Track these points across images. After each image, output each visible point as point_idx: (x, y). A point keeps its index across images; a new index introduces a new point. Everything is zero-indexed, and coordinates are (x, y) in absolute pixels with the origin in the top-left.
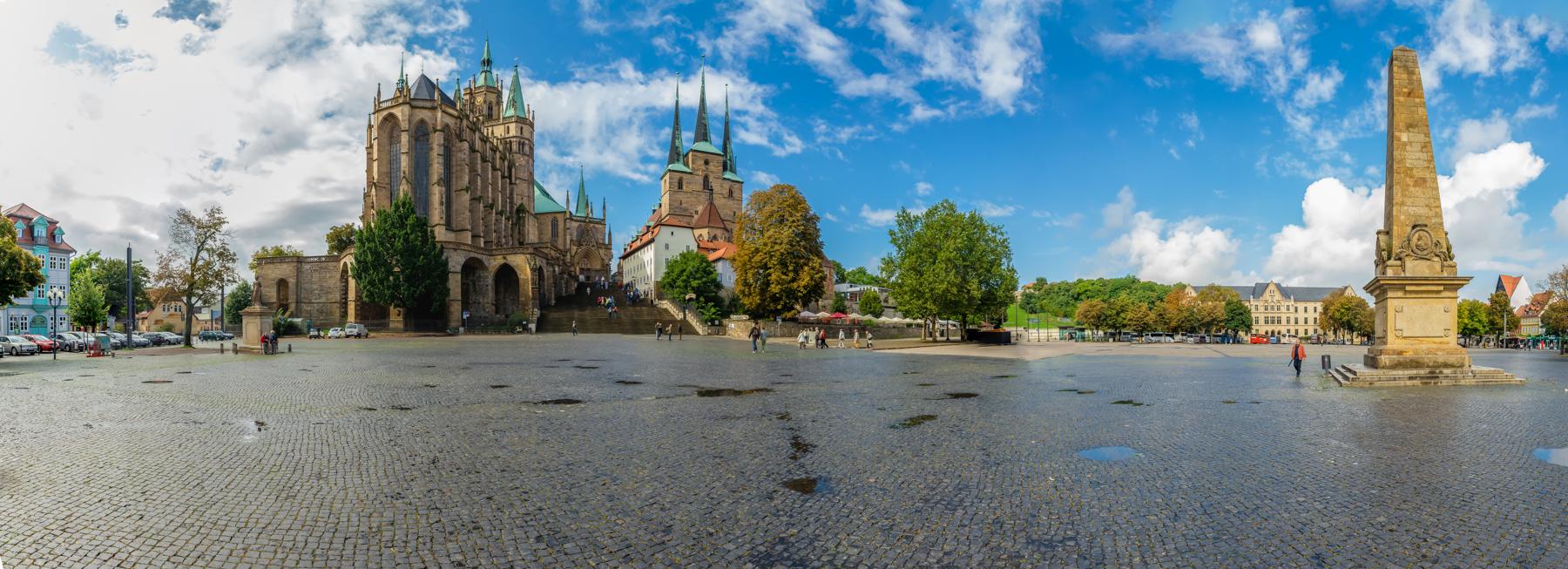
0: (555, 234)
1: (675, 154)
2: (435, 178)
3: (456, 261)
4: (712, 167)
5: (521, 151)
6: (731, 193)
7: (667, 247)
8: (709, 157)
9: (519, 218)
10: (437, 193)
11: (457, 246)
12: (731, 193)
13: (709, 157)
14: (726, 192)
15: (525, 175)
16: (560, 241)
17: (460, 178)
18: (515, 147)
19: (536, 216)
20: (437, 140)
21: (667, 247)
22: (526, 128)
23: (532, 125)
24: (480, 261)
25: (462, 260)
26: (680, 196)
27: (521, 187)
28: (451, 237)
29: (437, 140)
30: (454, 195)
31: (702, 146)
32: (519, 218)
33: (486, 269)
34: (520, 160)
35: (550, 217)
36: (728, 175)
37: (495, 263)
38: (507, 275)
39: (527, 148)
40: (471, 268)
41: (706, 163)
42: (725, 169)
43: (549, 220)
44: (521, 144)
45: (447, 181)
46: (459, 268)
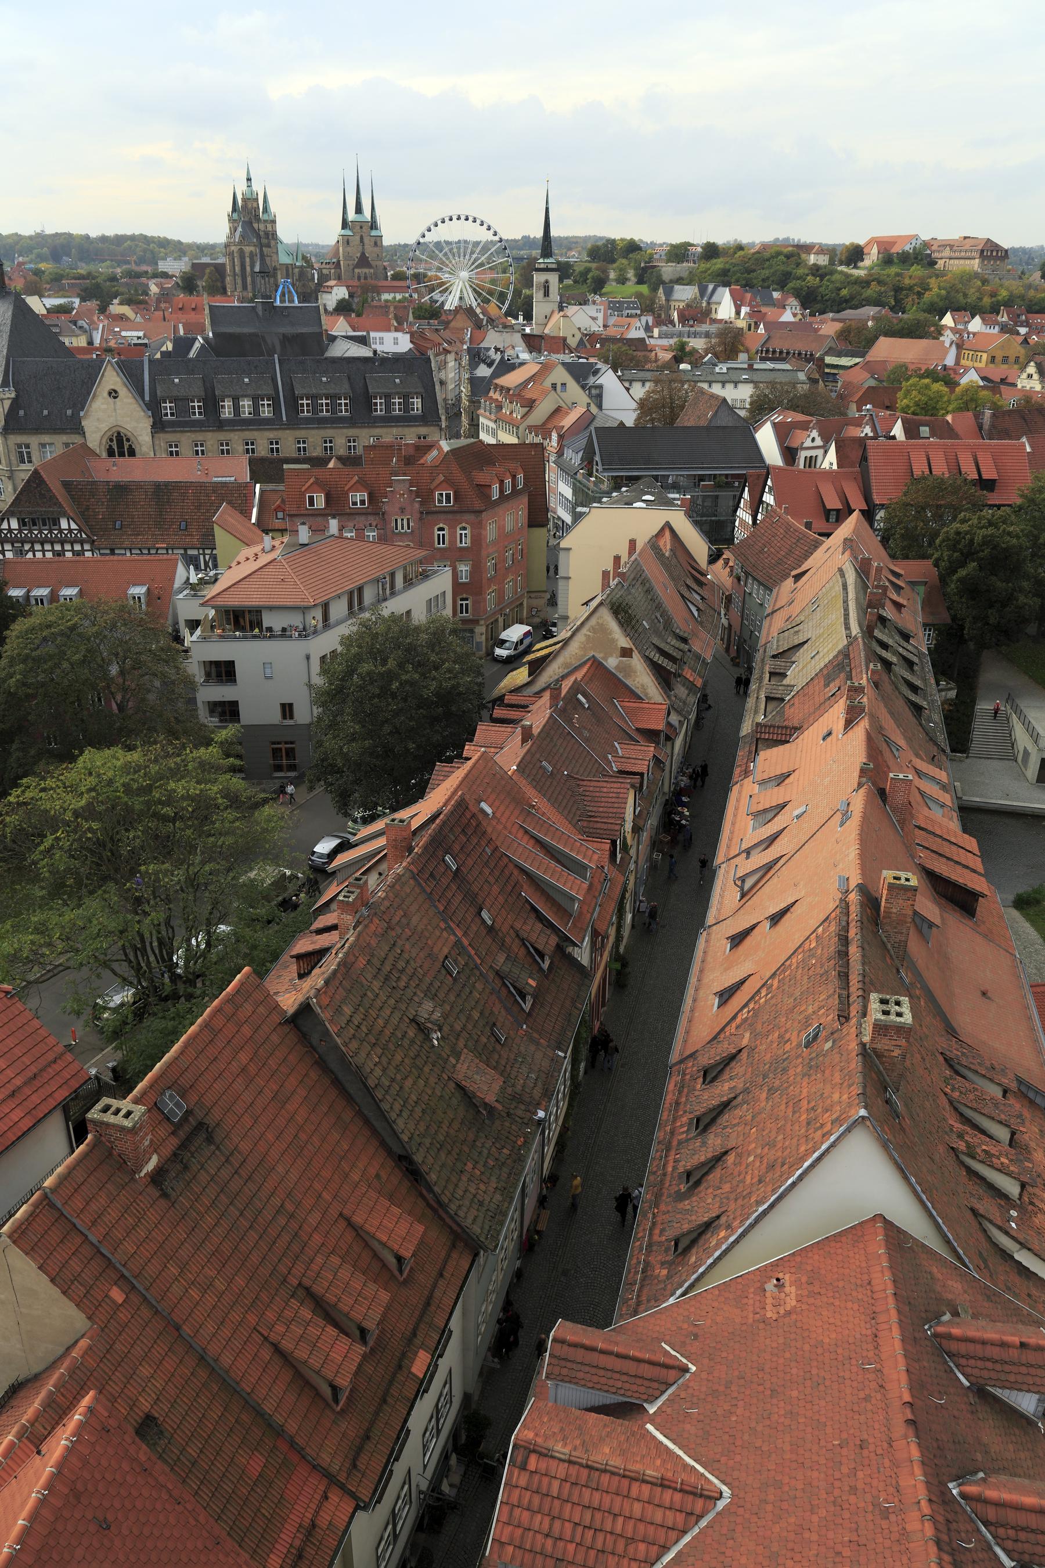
1: (345, 224)
4: (364, 230)
6: (376, 244)
12: (376, 244)
23: (274, 222)
26: (349, 249)
36: (374, 233)
42: (372, 228)
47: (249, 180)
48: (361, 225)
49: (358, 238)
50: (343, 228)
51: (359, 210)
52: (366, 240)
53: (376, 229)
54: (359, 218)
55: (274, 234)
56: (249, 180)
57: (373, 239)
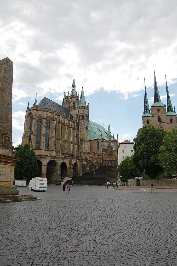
0: (98, 147)
1: (146, 110)
2: (42, 134)
3: (45, 162)
4: (161, 112)
5: (83, 119)
7: (123, 151)
8: (159, 108)
9: (81, 144)
10: (43, 139)
11: (46, 157)
12: (171, 121)
13: (159, 108)
14: (169, 121)
15: (84, 127)
16: (99, 149)
17: (52, 133)
18: (81, 118)
19: (90, 141)
20: (44, 121)
21: (123, 151)
22: (84, 110)
23: (88, 108)
24: (55, 161)
25: (48, 161)
27: (83, 132)
28: (47, 153)
29: (44, 121)
30: (50, 138)
31: (157, 104)
32: (81, 144)
33: (57, 163)
34: (82, 122)
35: (96, 141)
36: (169, 113)
37: (59, 162)
38: (63, 165)
39: (85, 117)
40: (52, 164)
41: (159, 110)
42: (168, 111)
43: (95, 143)
44: (83, 116)
45: (47, 135)
46: (46, 164)
47: (74, 86)
48: (159, 108)
49: (156, 118)
50: (144, 113)
51: (157, 99)
52: (163, 119)
53: (171, 110)
54: (157, 104)
55: (87, 116)
56: (74, 86)
57: (169, 118)
